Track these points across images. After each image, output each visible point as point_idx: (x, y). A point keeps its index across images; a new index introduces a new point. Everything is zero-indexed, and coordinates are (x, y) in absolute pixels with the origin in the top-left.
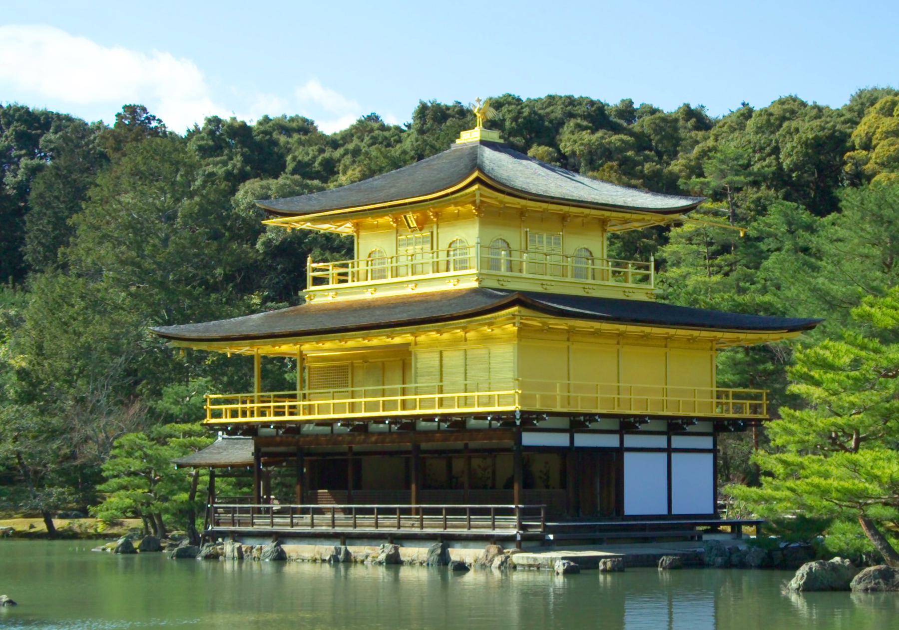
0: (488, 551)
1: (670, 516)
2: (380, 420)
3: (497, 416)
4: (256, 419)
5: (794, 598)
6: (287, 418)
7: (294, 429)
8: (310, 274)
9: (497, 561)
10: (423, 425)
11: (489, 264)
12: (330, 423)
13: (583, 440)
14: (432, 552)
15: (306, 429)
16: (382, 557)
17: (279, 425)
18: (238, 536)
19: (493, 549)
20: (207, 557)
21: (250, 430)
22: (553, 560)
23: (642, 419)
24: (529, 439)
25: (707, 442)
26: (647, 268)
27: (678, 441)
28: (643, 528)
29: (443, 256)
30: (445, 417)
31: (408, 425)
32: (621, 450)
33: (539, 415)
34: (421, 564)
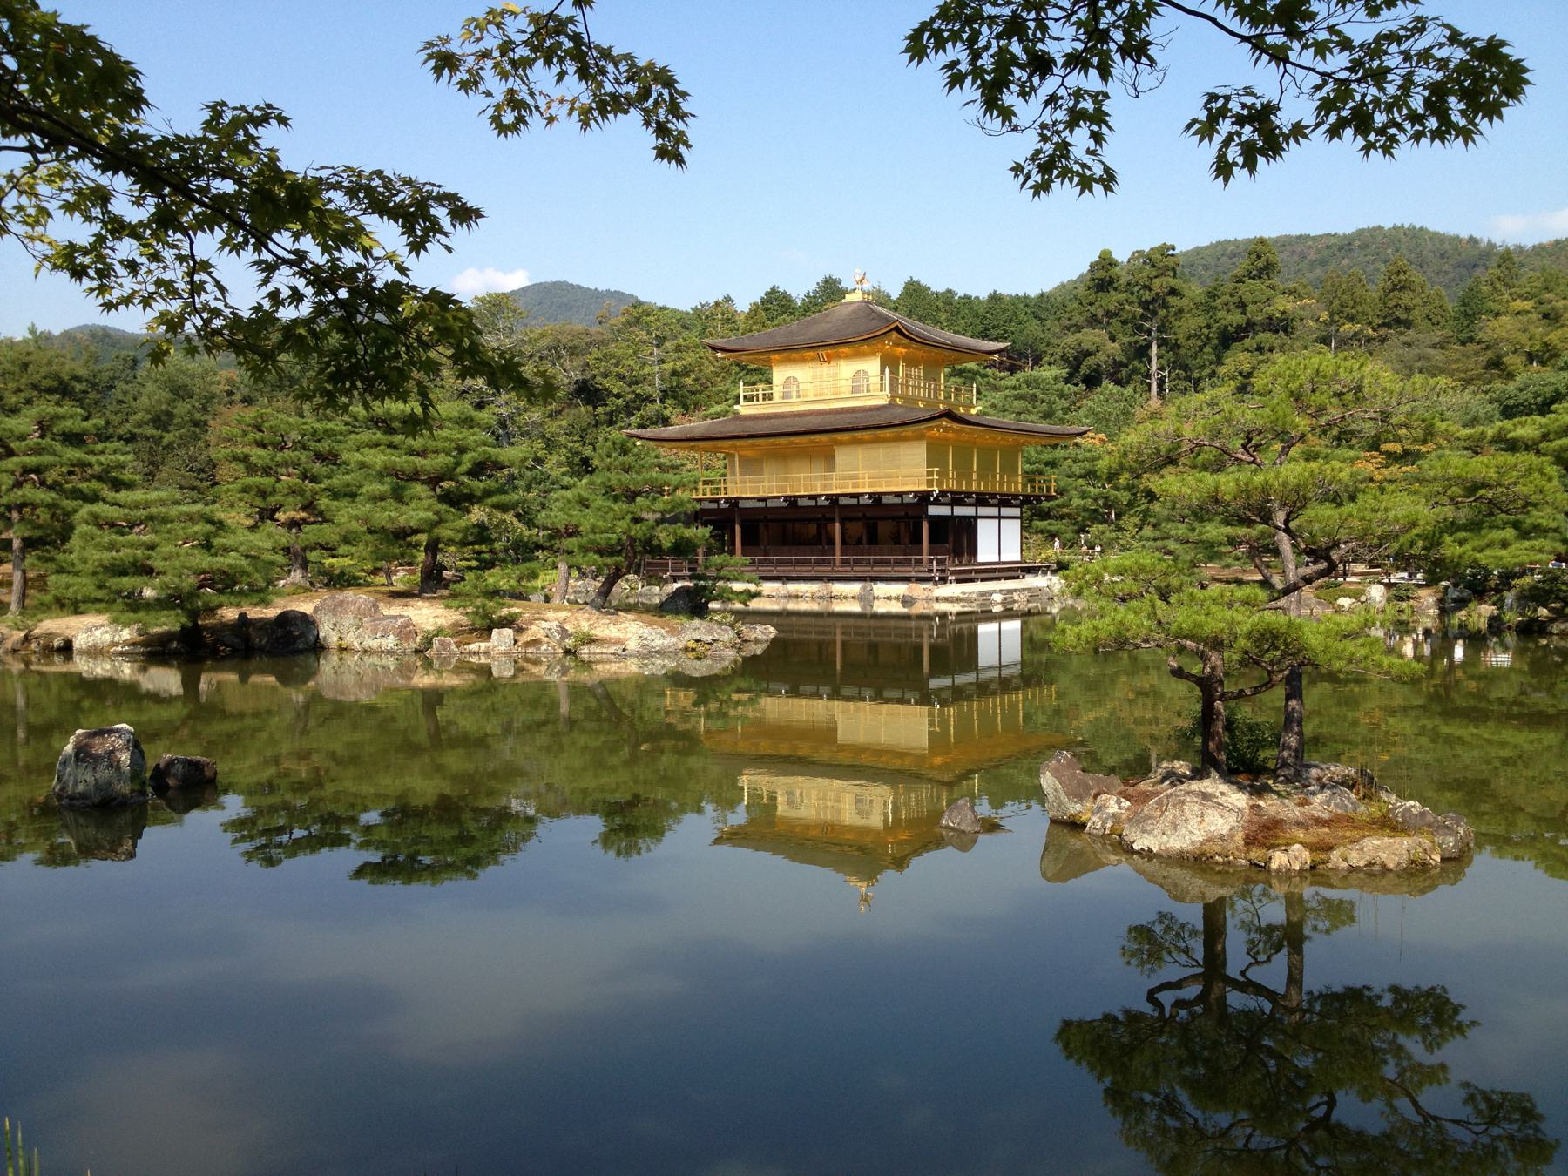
3: (916, 494)
7: (734, 502)
10: (844, 501)
11: (892, 389)
13: (960, 511)
14: (864, 588)
15: (742, 504)
17: (727, 500)
19: (913, 585)
22: (991, 593)
23: (993, 496)
24: (933, 510)
25: (1016, 512)
27: (1005, 511)
28: (994, 571)
30: (871, 495)
31: (834, 499)
32: (976, 518)
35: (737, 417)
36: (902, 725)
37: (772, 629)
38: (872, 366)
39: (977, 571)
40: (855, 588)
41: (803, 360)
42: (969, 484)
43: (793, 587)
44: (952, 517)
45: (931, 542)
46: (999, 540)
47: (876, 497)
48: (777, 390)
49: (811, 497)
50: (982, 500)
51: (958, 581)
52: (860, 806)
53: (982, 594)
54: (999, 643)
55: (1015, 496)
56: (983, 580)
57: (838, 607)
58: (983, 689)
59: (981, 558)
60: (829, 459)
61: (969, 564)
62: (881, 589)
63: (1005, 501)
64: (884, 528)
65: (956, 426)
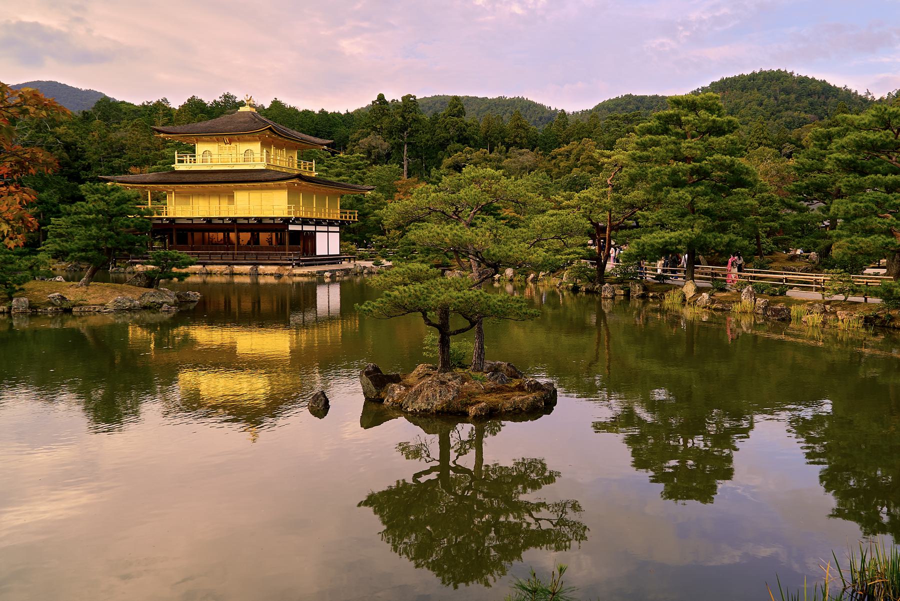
1: (328, 255)
3: (282, 219)
7: (172, 220)
8: (176, 158)
9: (286, 273)
11: (268, 160)
12: (191, 219)
13: (306, 228)
14: (252, 269)
16: (228, 271)
17: (167, 219)
19: (281, 268)
23: (325, 220)
24: (291, 228)
25: (337, 229)
27: (331, 229)
30: (256, 218)
31: (234, 220)
32: (315, 232)
35: (174, 172)
36: (275, 342)
38: (256, 147)
41: (214, 141)
42: (312, 213)
44: (302, 231)
45: (290, 244)
46: (328, 243)
47: (259, 220)
48: (198, 158)
49: (220, 219)
50: (318, 222)
52: (253, 387)
53: (319, 272)
54: (328, 298)
55: (337, 221)
56: (320, 264)
57: (237, 279)
58: (319, 322)
60: (231, 197)
63: (331, 223)
64: (263, 237)
65: (304, 183)
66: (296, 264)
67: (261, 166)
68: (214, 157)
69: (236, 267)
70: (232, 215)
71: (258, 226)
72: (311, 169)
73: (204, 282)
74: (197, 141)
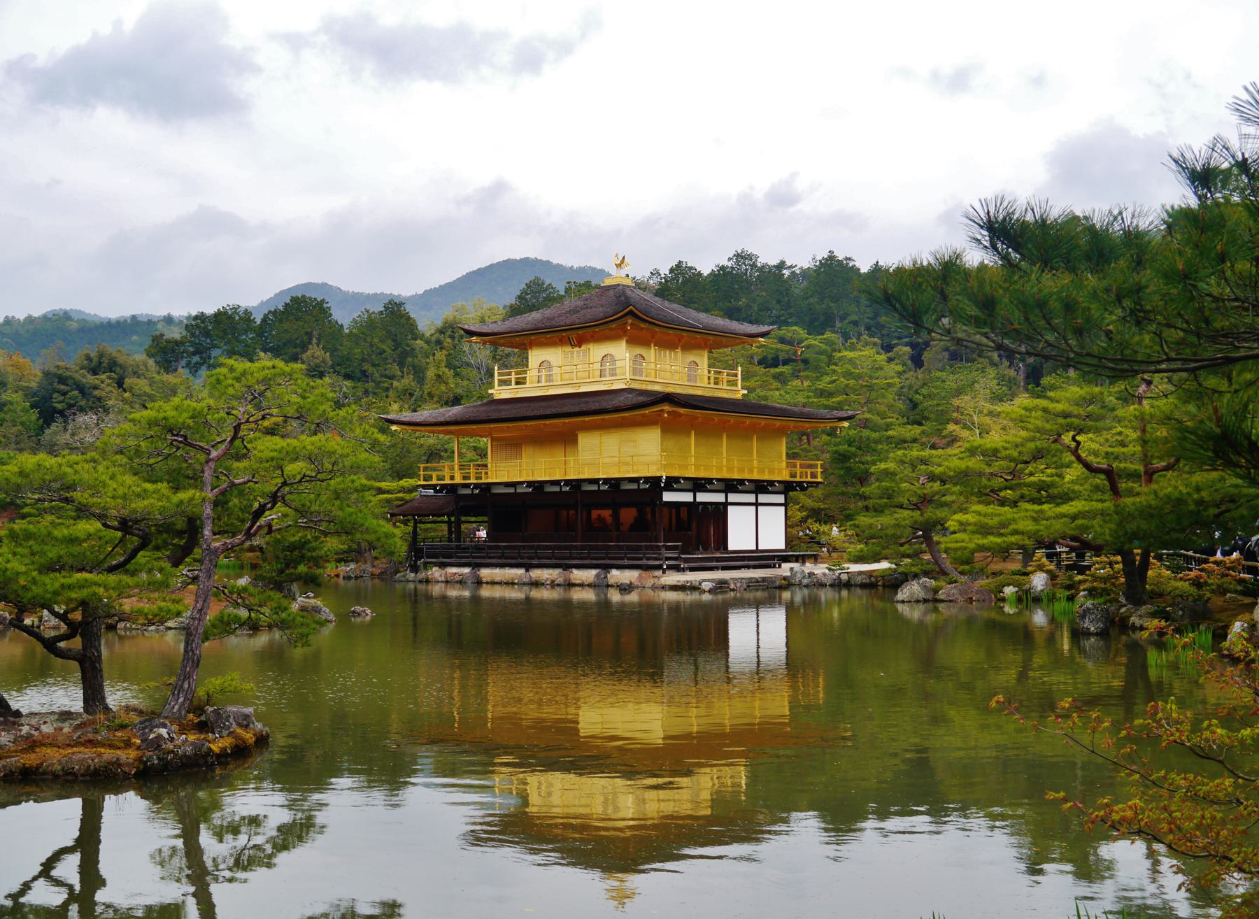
0: (640, 577)
1: (757, 550)
2: (555, 483)
3: (647, 479)
4: (458, 480)
5: (900, 607)
6: (484, 481)
9: (650, 582)
11: (635, 371)
13: (703, 497)
14: (597, 576)
16: (560, 580)
17: (476, 486)
18: (443, 565)
19: (644, 574)
20: (421, 581)
21: (452, 489)
23: (741, 482)
24: (668, 497)
25: (780, 499)
26: (736, 375)
27: (763, 498)
28: (743, 559)
29: (597, 366)
30: (606, 481)
31: (576, 484)
33: (676, 480)
34: (589, 585)
37: (368, 611)
39: (718, 559)
40: (589, 575)
43: (536, 574)
44: (694, 504)
46: (755, 527)
47: (614, 483)
50: (731, 486)
51: (692, 569)
54: (758, 635)
56: (724, 568)
57: (578, 595)
59: (731, 548)
61: (717, 549)
62: (616, 575)
63: (761, 487)
65: (682, 411)
66: (670, 567)
67: (624, 386)
68: (555, 370)
69: (575, 572)
70: (572, 476)
71: (615, 492)
72: (734, 383)
73: (528, 599)
74: (532, 345)
